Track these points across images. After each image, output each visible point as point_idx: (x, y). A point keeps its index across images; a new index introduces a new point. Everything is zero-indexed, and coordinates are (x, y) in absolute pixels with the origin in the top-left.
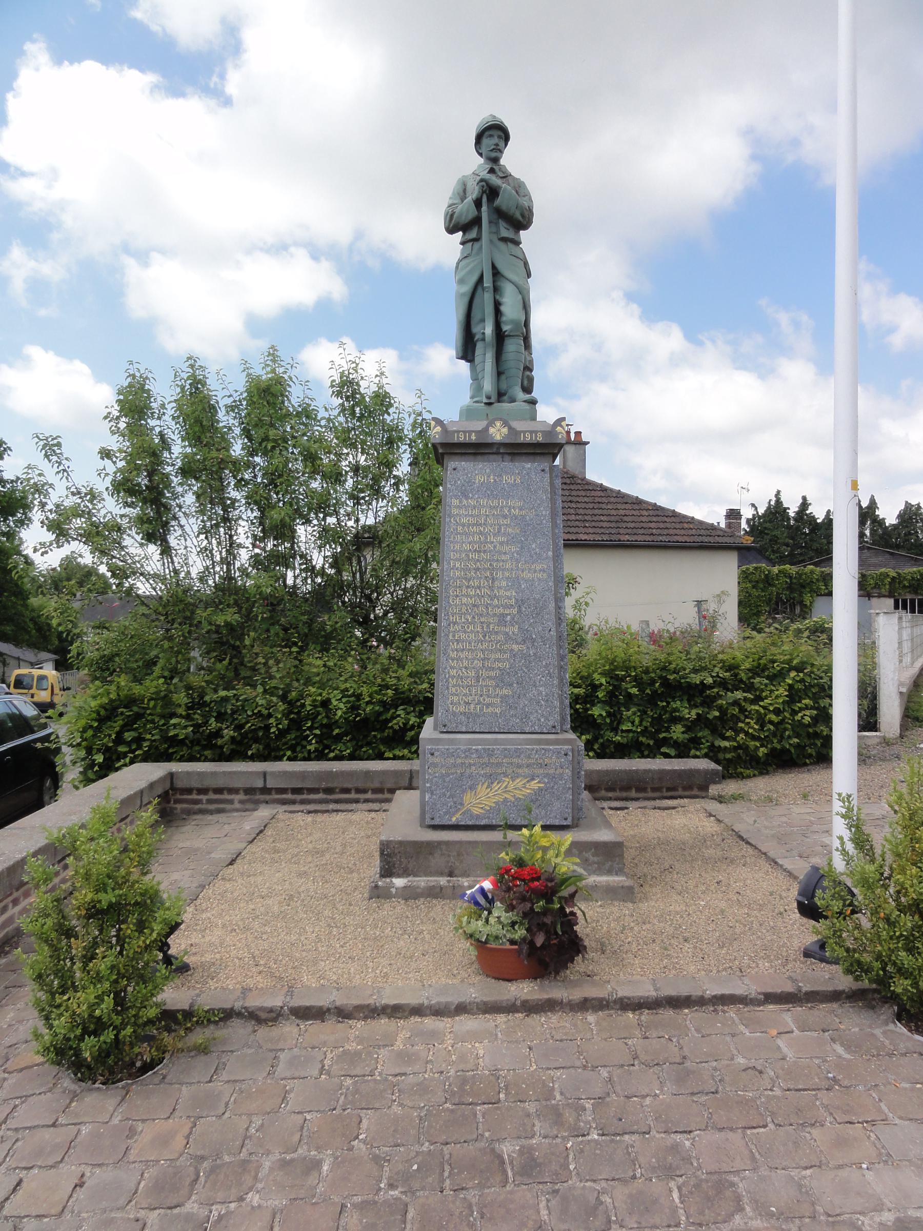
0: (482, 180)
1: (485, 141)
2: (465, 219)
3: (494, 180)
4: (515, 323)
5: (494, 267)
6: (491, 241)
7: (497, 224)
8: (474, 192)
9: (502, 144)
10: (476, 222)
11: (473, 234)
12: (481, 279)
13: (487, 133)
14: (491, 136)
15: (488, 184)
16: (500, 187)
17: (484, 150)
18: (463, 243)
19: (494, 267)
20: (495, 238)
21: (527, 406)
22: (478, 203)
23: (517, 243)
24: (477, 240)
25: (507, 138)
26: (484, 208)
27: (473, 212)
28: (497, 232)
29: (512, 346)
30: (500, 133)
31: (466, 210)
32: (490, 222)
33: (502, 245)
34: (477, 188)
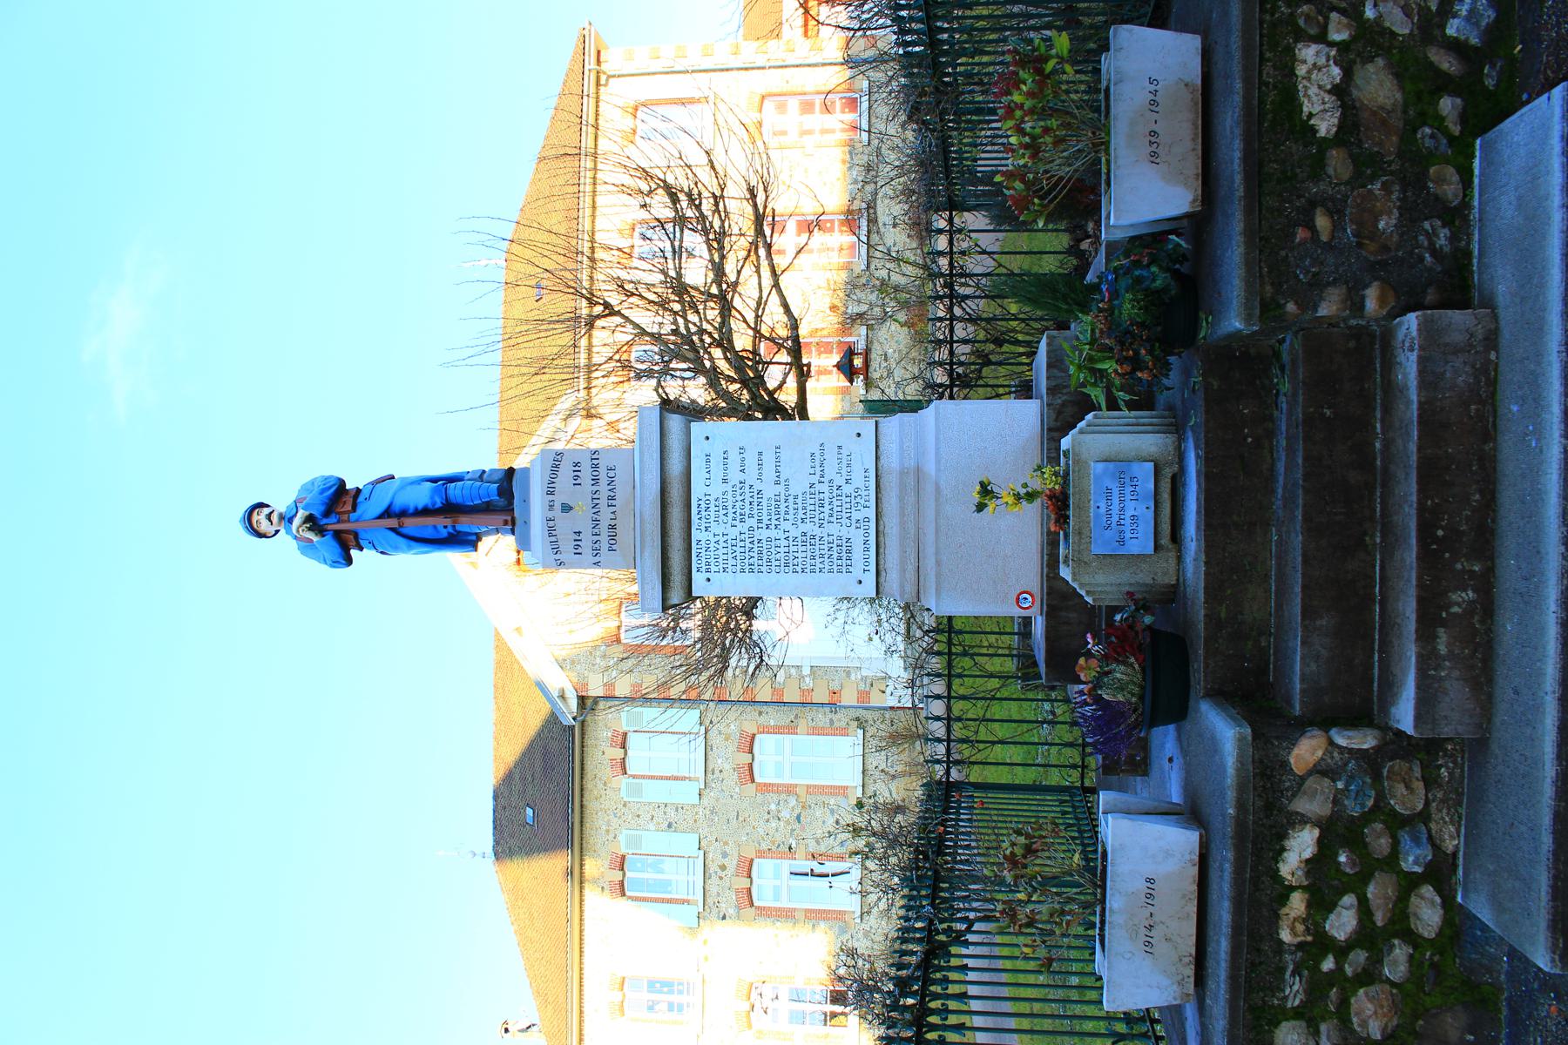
2: (336, 549)
6: (357, 521)
9: (266, 511)
10: (338, 536)
18: (361, 549)
19: (381, 517)
20: (353, 516)
23: (358, 491)
31: (327, 544)
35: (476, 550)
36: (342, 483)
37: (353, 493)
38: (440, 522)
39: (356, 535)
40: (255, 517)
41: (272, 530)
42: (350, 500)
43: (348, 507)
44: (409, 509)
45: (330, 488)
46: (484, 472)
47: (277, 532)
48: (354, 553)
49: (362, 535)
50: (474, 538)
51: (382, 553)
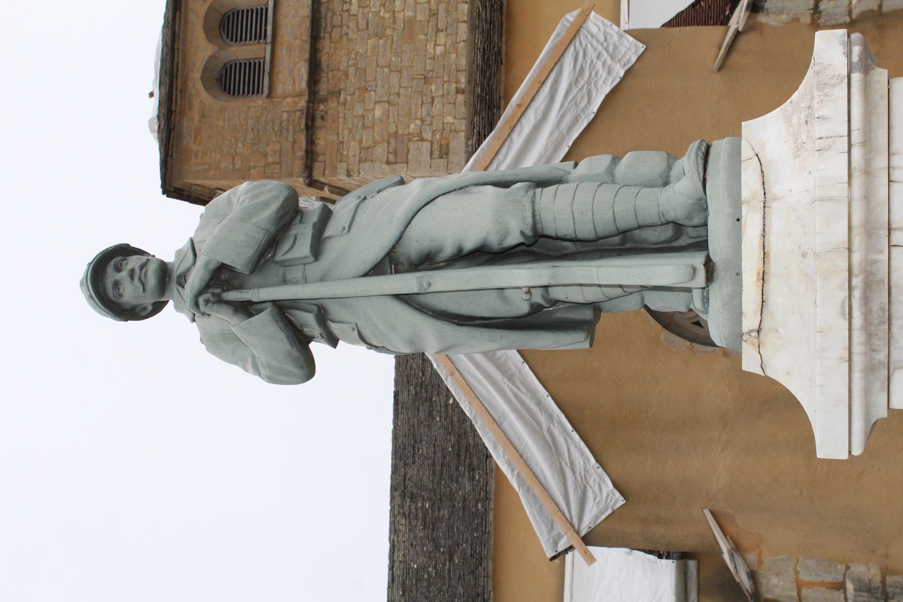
2: (281, 342)
3: (195, 279)
5: (376, 270)
6: (322, 279)
7: (285, 264)
9: (134, 262)
11: (308, 320)
12: (403, 298)
13: (110, 292)
14: (116, 284)
15: (200, 293)
16: (207, 264)
18: (333, 341)
19: (376, 270)
20: (316, 269)
22: (246, 309)
25: (124, 251)
27: (264, 318)
30: (110, 269)
32: (284, 282)
33: (332, 250)
39: (323, 317)
40: (111, 276)
41: (148, 301)
43: (303, 248)
44: (439, 251)
45: (266, 204)
47: (158, 307)
48: (318, 348)
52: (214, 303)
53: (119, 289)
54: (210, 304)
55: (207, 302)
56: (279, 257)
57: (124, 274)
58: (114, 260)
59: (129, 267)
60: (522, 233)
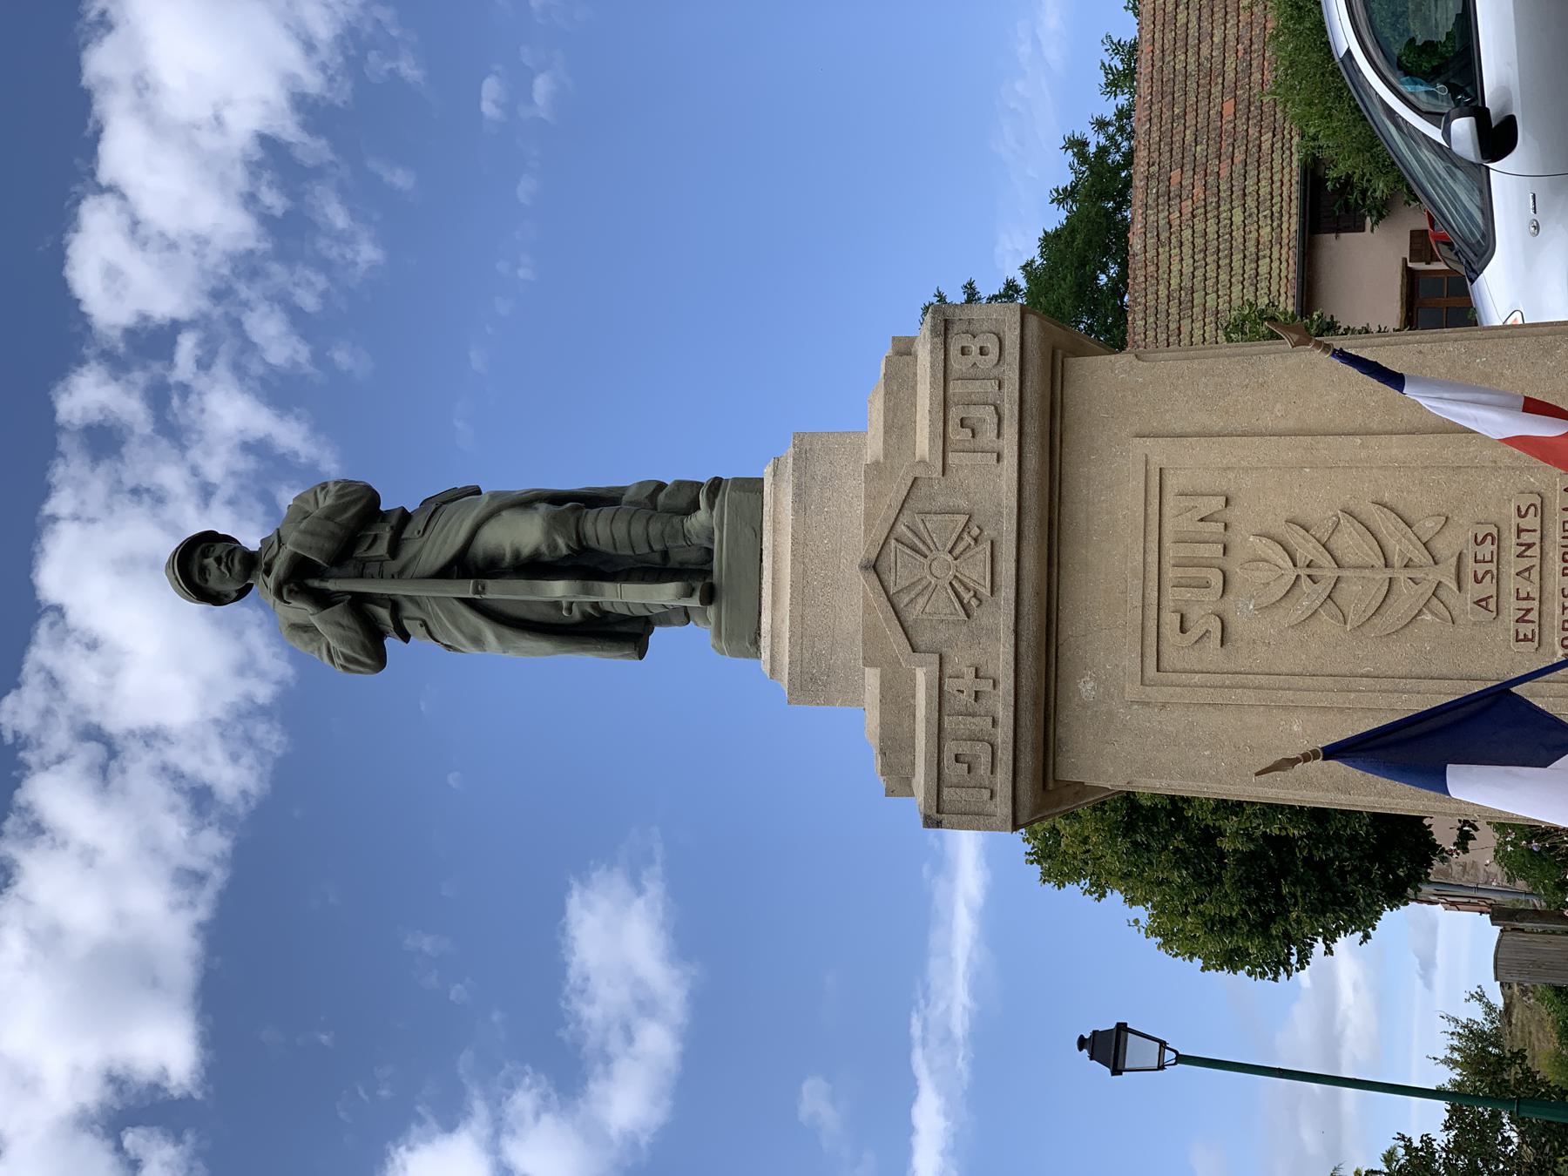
0: (278, 593)
1: (213, 584)
3: (279, 567)
4: (553, 524)
7: (364, 562)
8: (302, 611)
9: (220, 549)
10: (359, 605)
11: (384, 614)
12: (469, 603)
14: (203, 570)
17: (232, 587)
18: (405, 636)
20: (394, 566)
21: (725, 498)
22: (323, 600)
23: (405, 517)
24: (395, 606)
26: (332, 585)
28: (381, 561)
29: (601, 529)
31: (331, 628)
32: (361, 576)
33: (407, 553)
34: (294, 603)
35: (641, 656)
36: (374, 498)
37: (394, 520)
38: (558, 589)
42: (386, 534)
43: (382, 548)
44: (502, 557)
45: (354, 502)
46: (661, 486)
47: (242, 593)
48: (392, 643)
49: (409, 610)
50: (638, 629)
51: (448, 647)
52: (297, 593)
53: (205, 574)
54: (293, 594)
55: (290, 591)
56: (360, 553)
57: (210, 561)
58: (204, 545)
59: (217, 553)
60: (568, 546)
